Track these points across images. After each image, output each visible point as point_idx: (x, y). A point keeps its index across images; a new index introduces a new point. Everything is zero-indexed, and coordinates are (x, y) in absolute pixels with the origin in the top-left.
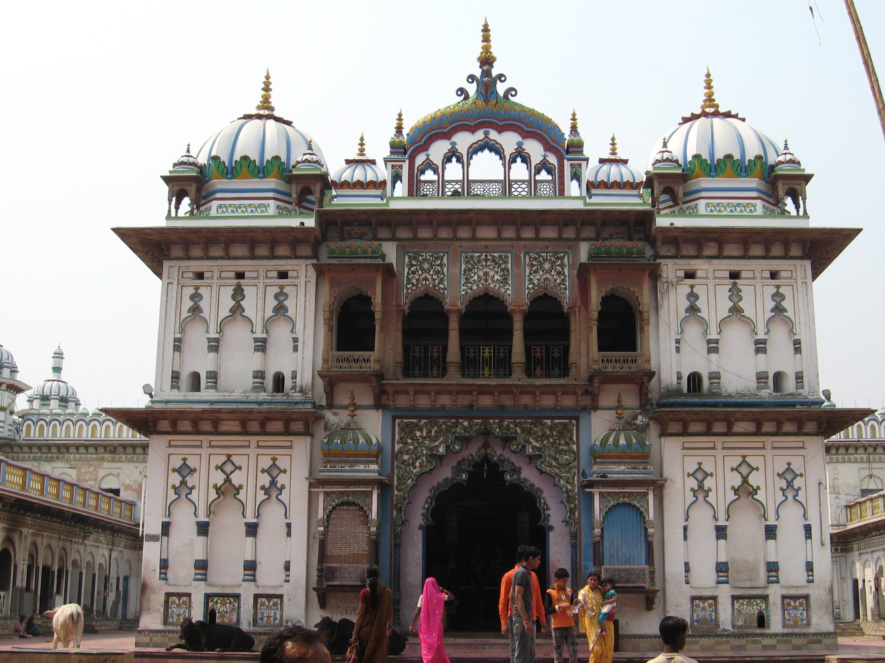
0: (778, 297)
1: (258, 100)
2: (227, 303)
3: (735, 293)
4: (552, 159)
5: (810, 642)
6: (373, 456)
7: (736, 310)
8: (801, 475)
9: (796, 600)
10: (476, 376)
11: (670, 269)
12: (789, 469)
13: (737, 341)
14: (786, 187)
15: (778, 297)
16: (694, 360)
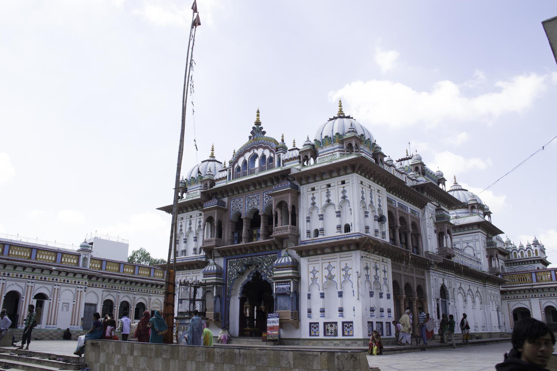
0: (344, 192)
1: (210, 154)
2: (188, 226)
3: (328, 195)
4: (272, 155)
5: (352, 343)
6: (214, 274)
7: (329, 201)
8: (351, 268)
9: (347, 325)
10: (252, 241)
11: (305, 189)
12: (347, 267)
13: (331, 213)
14: (347, 143)
15: (344, 192)
16: (317, 224)
